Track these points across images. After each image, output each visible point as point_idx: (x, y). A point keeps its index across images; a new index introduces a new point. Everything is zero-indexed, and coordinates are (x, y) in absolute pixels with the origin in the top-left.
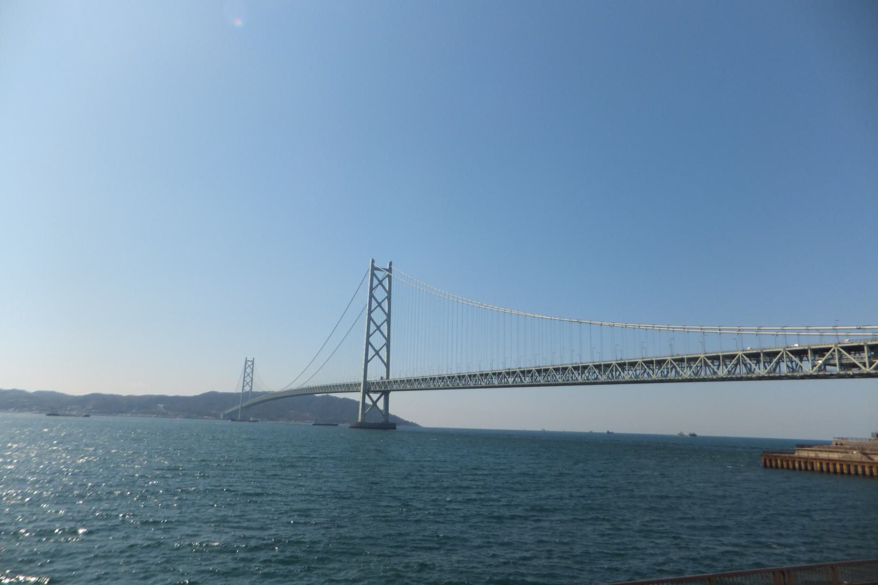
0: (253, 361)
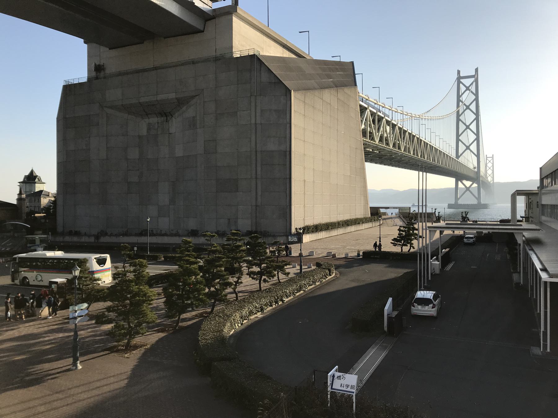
0: (493, 157)
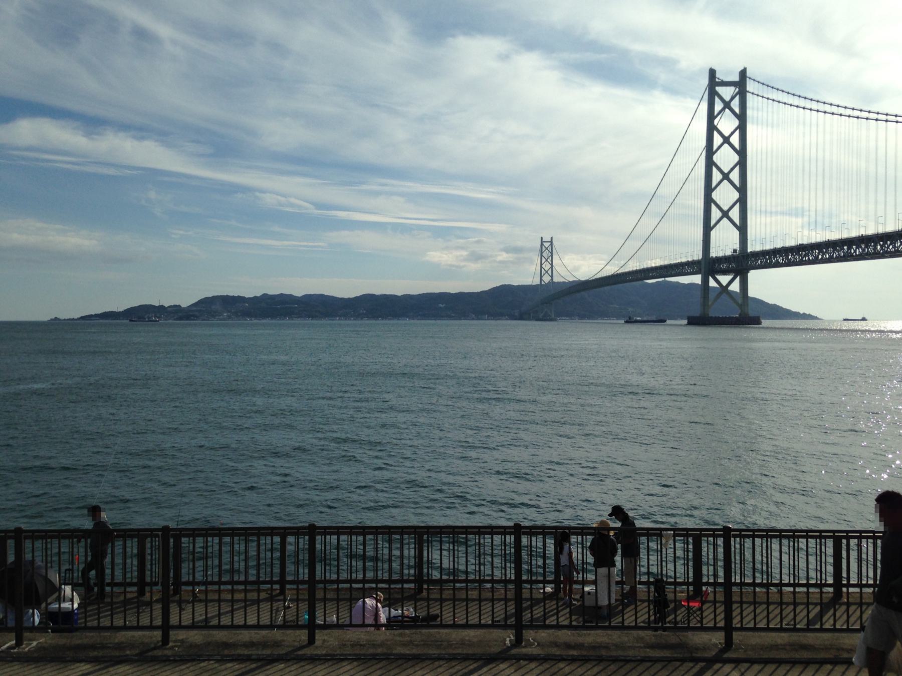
0: (551, 242)
